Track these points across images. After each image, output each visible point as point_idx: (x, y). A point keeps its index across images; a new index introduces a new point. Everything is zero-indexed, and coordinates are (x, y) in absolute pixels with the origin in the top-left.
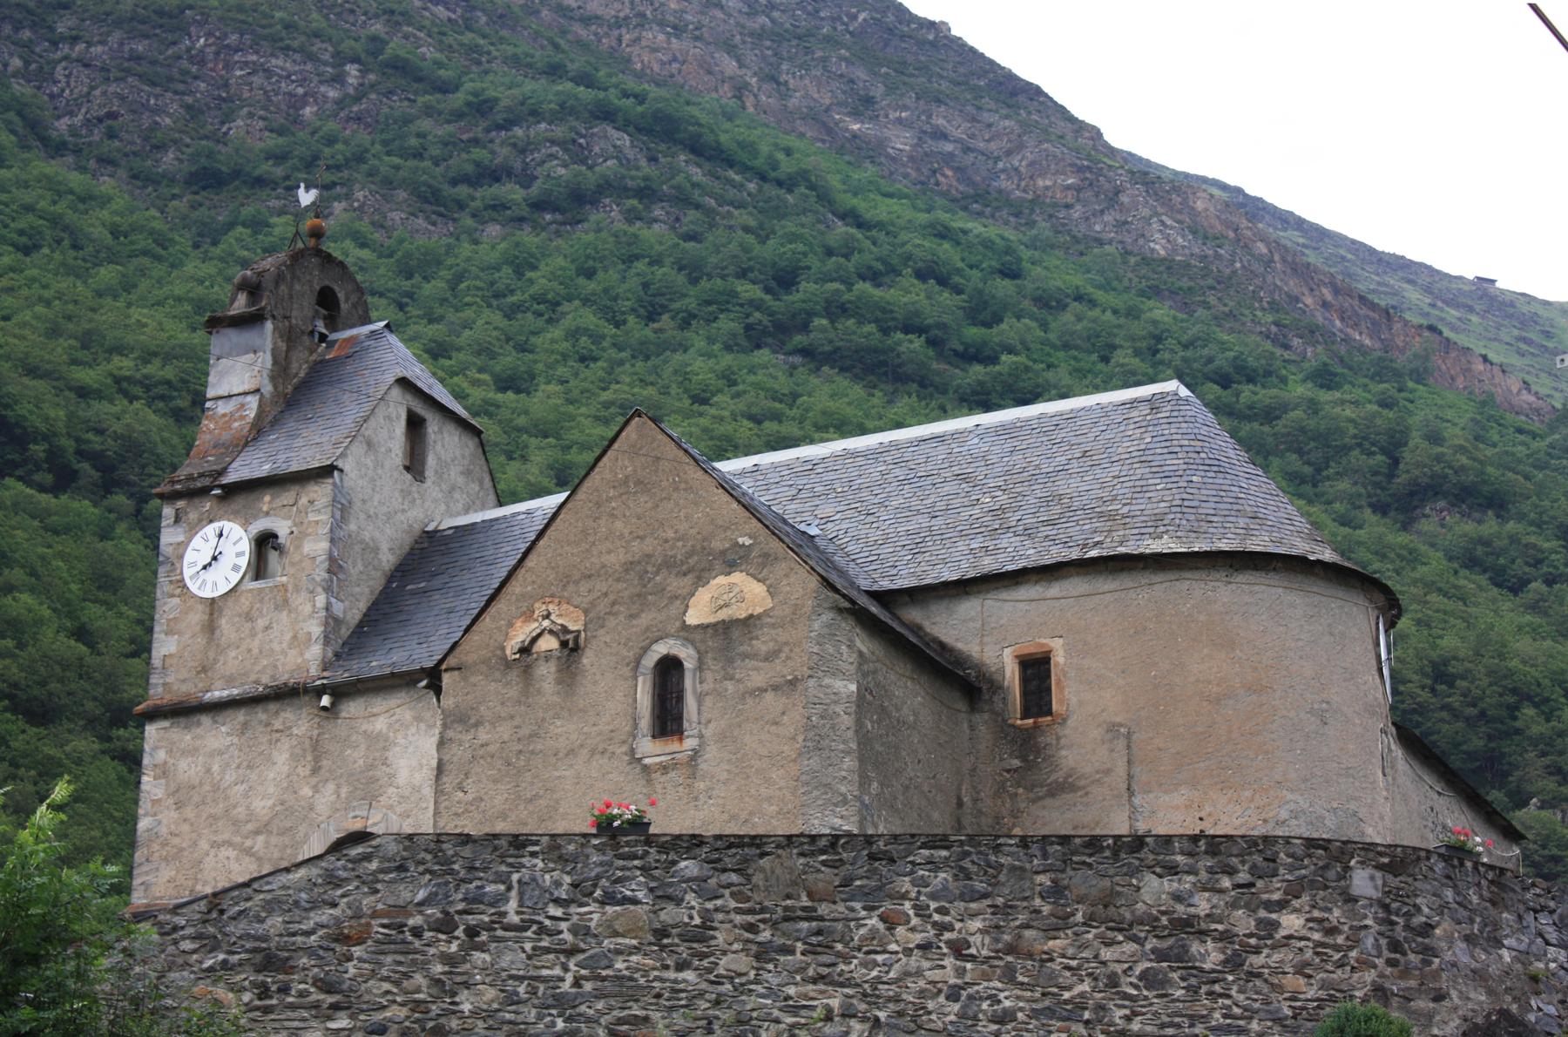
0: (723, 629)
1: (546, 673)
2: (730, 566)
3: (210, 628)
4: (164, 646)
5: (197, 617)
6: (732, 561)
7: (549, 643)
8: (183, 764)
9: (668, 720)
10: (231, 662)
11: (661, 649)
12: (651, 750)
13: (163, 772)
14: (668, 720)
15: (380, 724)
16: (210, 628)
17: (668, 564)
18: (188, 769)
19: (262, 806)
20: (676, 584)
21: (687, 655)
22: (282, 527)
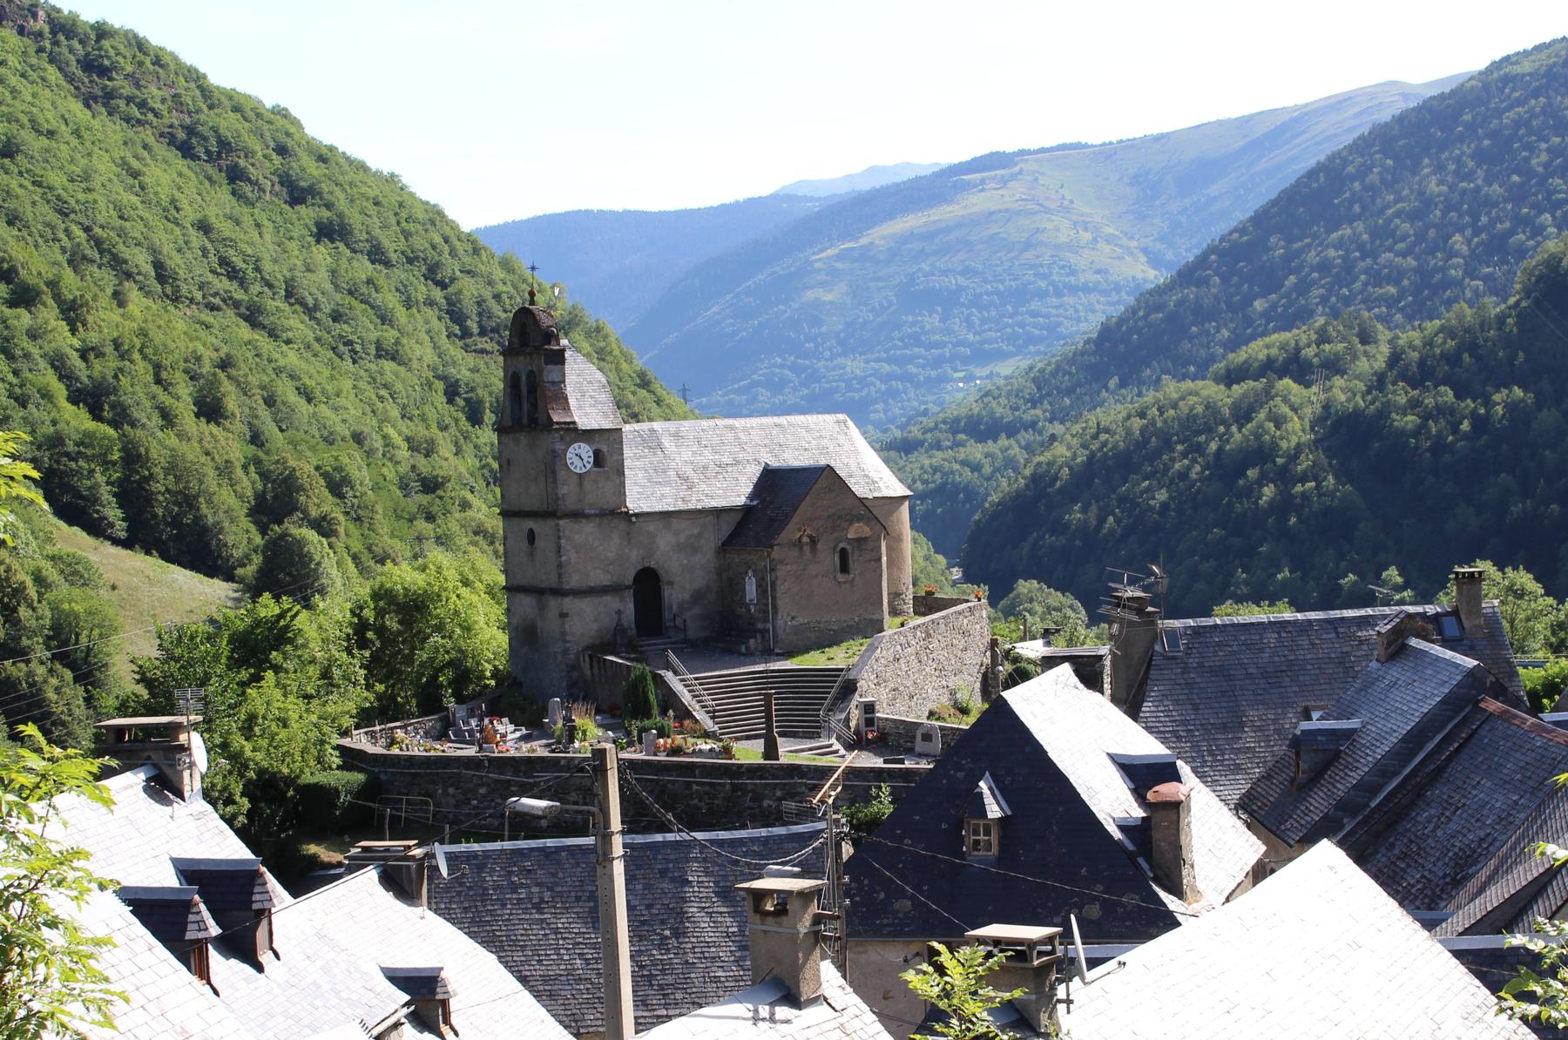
0: (859, 540)
1: (807, 549)
2: (859, 520)
3: (581, 485)
4: (563, 490)
5: (575, 480)
6: (859, 518)
7: (805, 539)
8: (577, 537)
9: (844, 568)
10: (590, 498)
11: (841, 545)
12: (841, 578)
13: (568, 539)
14: (844, 568)
15: (652, 528)
16: (581, 485)
17: (840, 517)
18: (577, 538)
19: (610, 555)
20: (844, 524)
21: (848, 547)
22: (604, 448)
